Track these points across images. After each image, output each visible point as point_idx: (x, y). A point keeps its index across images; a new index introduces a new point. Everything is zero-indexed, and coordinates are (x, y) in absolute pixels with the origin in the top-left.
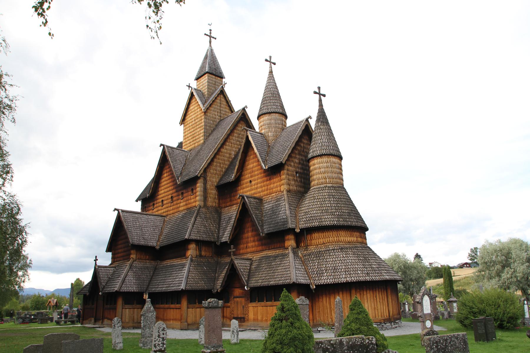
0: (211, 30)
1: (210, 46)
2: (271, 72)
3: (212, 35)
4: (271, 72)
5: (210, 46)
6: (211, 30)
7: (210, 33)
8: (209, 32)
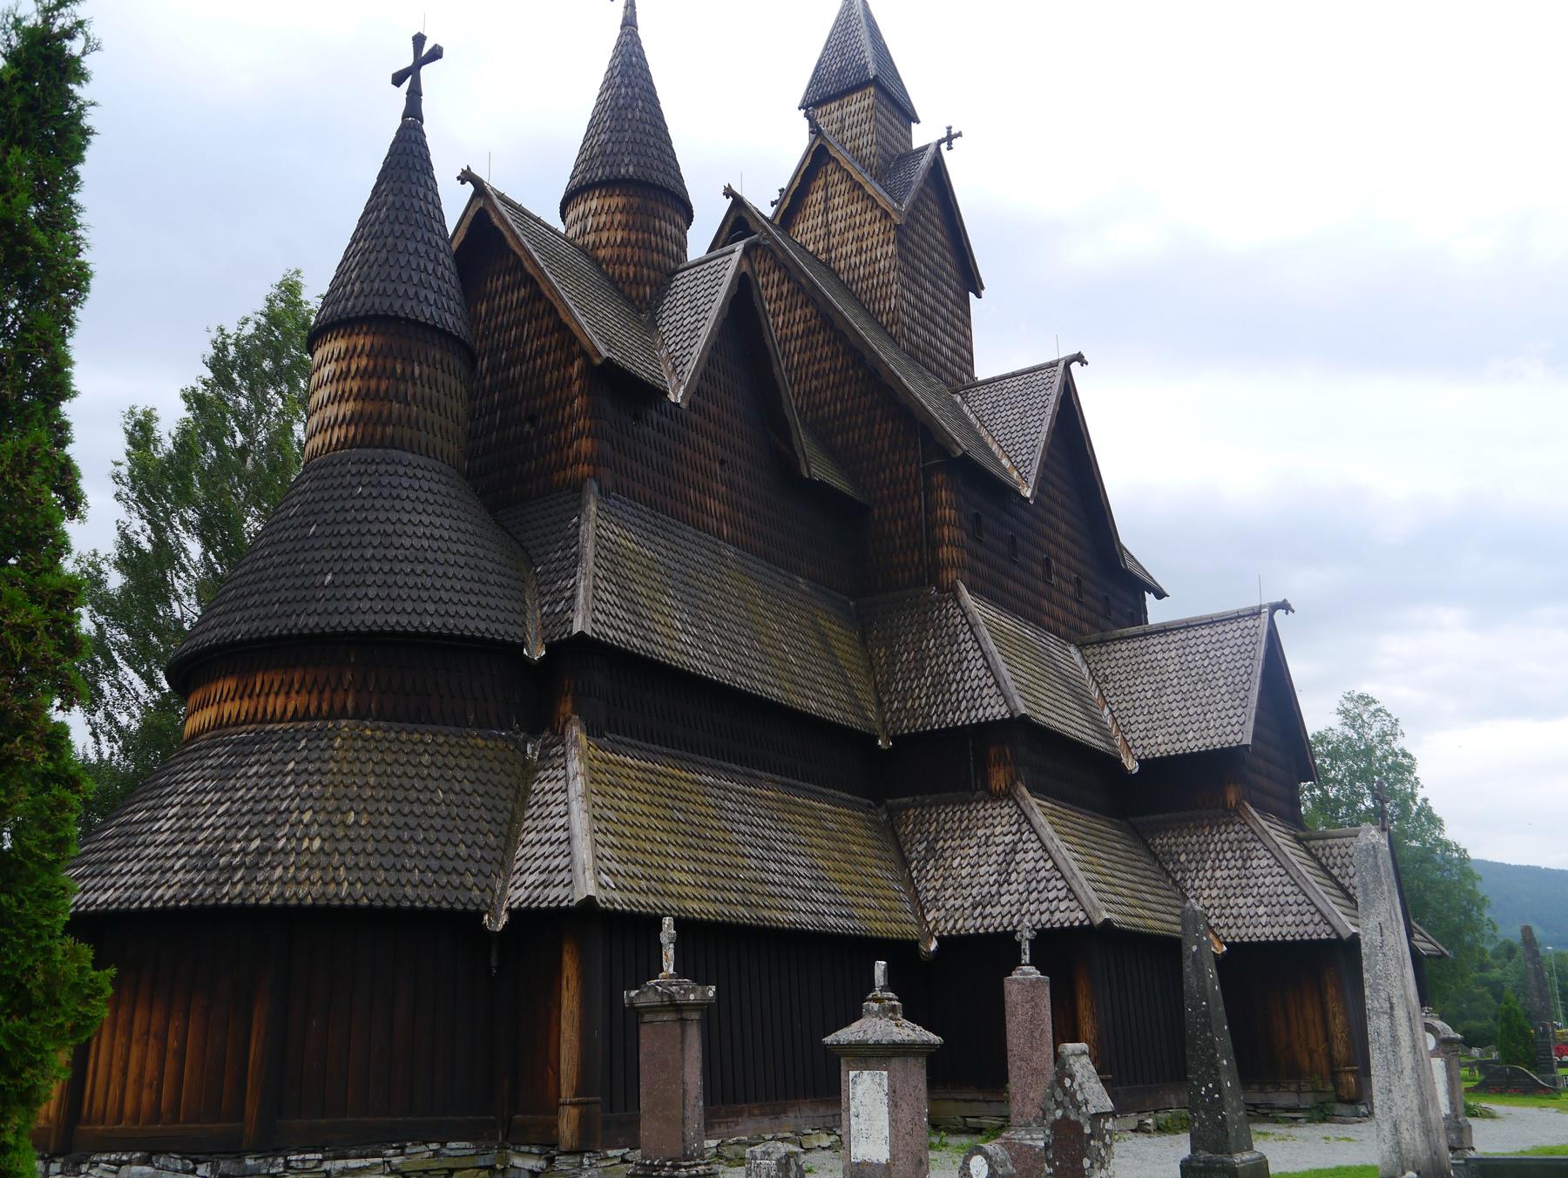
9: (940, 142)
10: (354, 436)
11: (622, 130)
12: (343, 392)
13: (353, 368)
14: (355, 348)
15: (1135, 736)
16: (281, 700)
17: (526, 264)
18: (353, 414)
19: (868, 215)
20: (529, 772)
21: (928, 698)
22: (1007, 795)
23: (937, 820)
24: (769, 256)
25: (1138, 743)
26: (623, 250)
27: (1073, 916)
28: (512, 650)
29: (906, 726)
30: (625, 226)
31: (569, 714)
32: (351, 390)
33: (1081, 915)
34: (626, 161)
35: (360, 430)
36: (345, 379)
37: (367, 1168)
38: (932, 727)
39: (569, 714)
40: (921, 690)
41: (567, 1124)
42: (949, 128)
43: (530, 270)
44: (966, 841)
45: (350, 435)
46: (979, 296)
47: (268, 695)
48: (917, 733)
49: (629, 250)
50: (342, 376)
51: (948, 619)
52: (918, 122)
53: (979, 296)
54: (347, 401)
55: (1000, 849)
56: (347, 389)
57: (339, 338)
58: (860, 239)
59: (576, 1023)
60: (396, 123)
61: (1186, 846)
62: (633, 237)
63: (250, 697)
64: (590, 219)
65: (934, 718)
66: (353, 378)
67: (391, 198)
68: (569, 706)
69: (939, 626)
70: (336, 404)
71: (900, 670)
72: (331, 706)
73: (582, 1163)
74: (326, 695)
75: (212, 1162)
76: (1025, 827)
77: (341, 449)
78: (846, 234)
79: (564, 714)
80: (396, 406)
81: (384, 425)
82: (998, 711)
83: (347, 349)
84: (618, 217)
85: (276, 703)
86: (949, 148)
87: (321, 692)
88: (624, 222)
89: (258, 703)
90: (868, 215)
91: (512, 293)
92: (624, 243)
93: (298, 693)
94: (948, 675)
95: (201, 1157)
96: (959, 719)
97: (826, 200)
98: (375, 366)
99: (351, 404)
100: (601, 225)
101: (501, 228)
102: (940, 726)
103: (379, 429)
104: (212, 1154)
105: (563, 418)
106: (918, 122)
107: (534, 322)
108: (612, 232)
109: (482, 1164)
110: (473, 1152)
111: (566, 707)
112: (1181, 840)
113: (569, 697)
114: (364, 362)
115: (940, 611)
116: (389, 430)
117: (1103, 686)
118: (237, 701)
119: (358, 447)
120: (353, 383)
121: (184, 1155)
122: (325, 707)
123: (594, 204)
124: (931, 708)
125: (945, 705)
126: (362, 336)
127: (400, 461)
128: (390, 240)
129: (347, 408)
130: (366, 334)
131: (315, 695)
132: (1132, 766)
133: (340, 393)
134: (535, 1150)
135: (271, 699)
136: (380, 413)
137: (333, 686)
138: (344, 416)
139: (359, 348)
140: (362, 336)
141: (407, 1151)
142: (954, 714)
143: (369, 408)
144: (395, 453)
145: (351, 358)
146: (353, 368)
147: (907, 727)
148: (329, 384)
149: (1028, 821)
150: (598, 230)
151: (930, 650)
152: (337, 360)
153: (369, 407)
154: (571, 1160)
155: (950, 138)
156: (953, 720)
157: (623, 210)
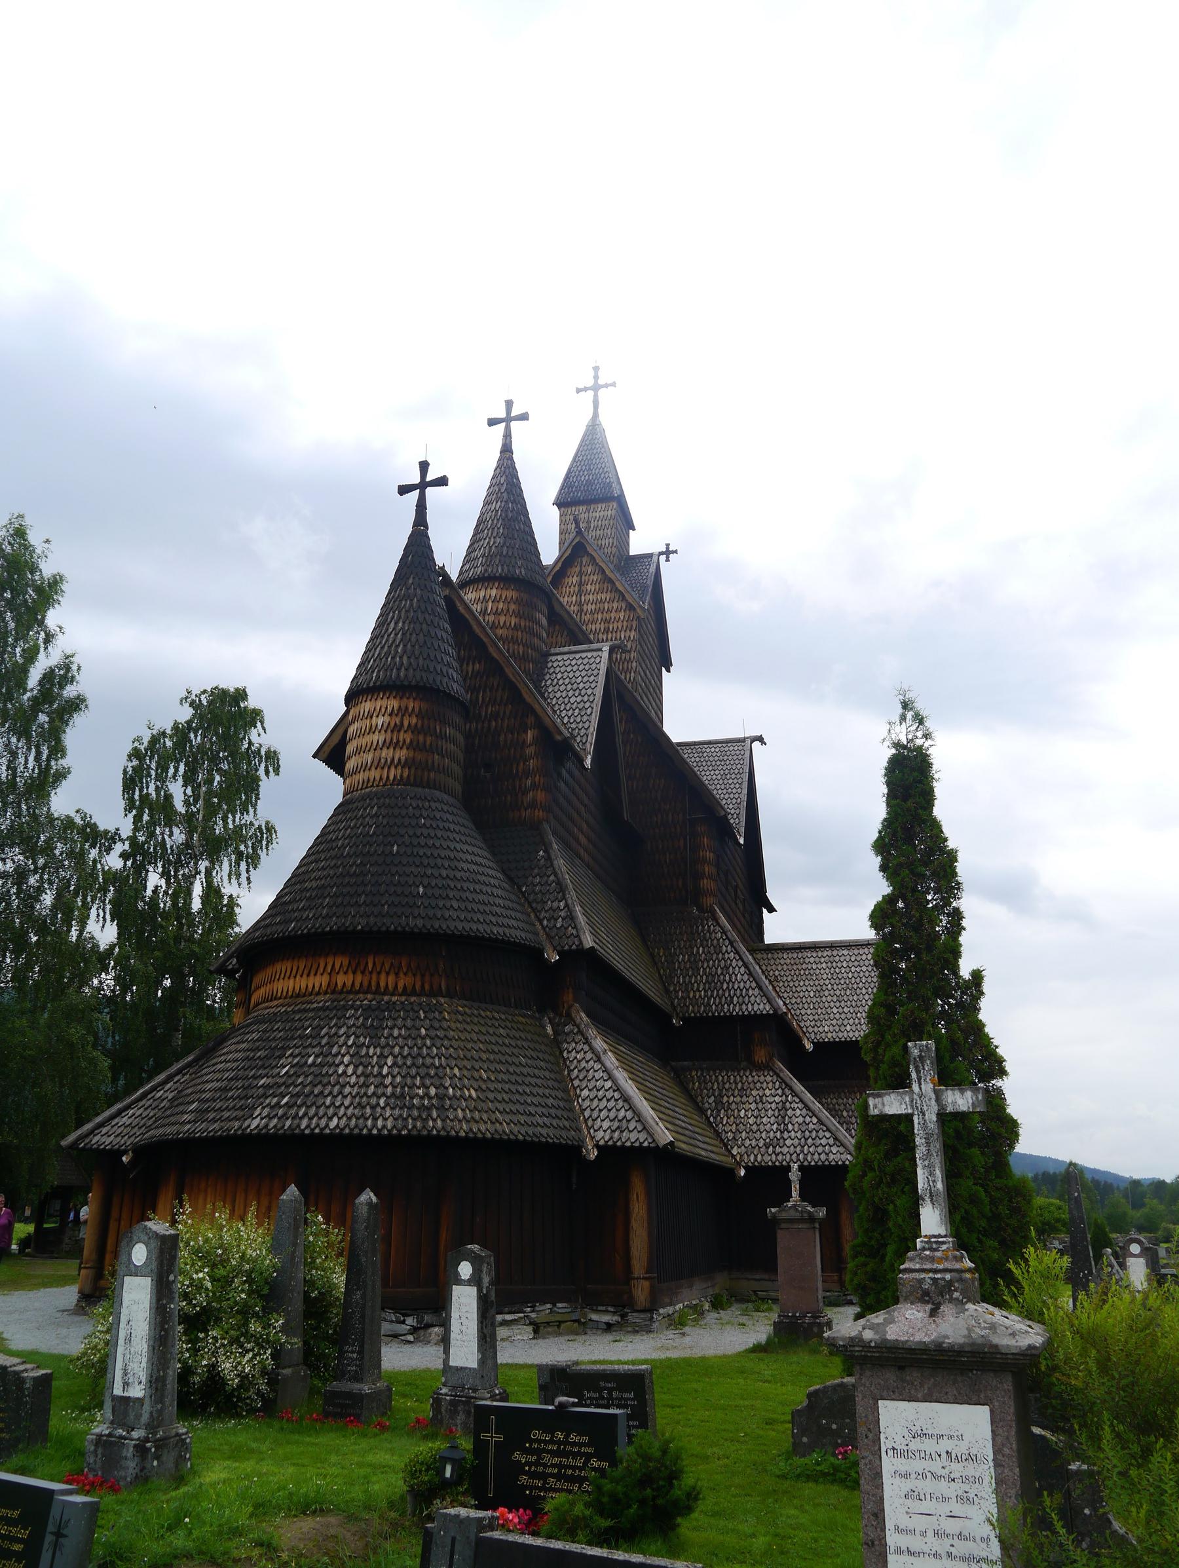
0: (596, 369)
1: (596, 415)
2: (507, 449)
3: (601, 382)
4: (507, 449)
5: (596, 415)
6: (596, 369)
7: (596, 377)
9: (661, 553)
10: (409, 776)
11: (513, 538)
12: (398, 741)
13: (406, 724)
14: (407, 708)
15: (808, 1024)
17: (491, 650)
18: (406, 759)
19: (615, 605)
20: (556, 1044)
21: (706, 991)
22: (767, 1067)
23: (717, 1081)
24: (565, 633)
25: (810, 1030)
26: (515, 632)
27: (844, 1157)
28: (536, 953)
30: (518, 615)
33: (849, 1157)
34: (519, 564)
35: (412, 772)
36: (399, 731)
37: (515, 1320)
38: (713, 1014)
40: (698, 985)
41: (641, 1291)
42: (668, 545)
43: (495, 655)
44: (745, 1099)
46: (668, 671)
47: (379, 973)
48: (702, 1017)
49: (520, 633)
50: (397, 728)
51: (710, 934)
52: (634, 530)
53: (668, 671)
54: (401, 748)
55: (774, 1106)
56: (401, 739)
57: (392, 697)
58: (607, 621)
59: (646, 1224)
61: (845, 1105)
62: (523, 624)
63: (363, 973)
64: (490, 604)
65: (714, 1007)
66: (405, 732)
67: (419, 592)
68: (571, 995)
69: (705, 938)
71: (679, 967)
72: (431, 986)
73: (652, 1318)
74: (427, 978)
75: (418, 1315)
76: (787, 1092)
77: (398, 785)
78: (596, 615)
80: (436, 757)
81: (429, 771)
82: (763, 1007)
84: (512, 606)
86: (667, 560)
87: (423, 976)
88: (517, 611)
90: (615, 605)
91: (468, 664)
92: (517, 628)
93: (405, 974)
94: (719, 976)
96: (734, 1010)
97: (580, 584)
98: (422, 726)
99: (404, 751)
100: (499, 610)
101: (467, 616)
102: (719, 1013)
103: (426, 774)
104: (416, 1310)
105: (517, 771)
106: (634, 530)
107: (488, 693)
109: (574, 1318)
110: (570, 1310)
111: (569, 997)
112: (840, 1101)
113: (571, 990)
114: (414, 721)
115: (703, 927)
116: (432, 775)
117: (775, 984)
118: (351, 976)
119: (411, 785)
121: (396, 1310)
122: (427, 987)
123: (494, 592)
124: (709, 999)
125: (720, 998)
126: (411, 700)
127: (426, 798)
128: (424, 626)
129: (402, 754)
130: (414, 699)
131: (418, 978)
132: (809, 1046)
134: (610, 1309)
135: (383, 976)
136: (427, 761)
137: (405, 970)
138: (400, 759)
139: (410, 709)
140: (411, 700)
141: (537, 1309)
142: (729, 1006)
143: (419, 756)
144: (437, 793)
145: (403, 716)
146: (406, 724)
147: (693, 1011)
148: (383, 732)
149: (791, 1089)
150: (496, 613)
151: (700, 955)
152: (390, 715)
153: (419, 756)
154: (642, 1316)
155: (668, 553)
156: (729, 1010)
157: (518, 601)
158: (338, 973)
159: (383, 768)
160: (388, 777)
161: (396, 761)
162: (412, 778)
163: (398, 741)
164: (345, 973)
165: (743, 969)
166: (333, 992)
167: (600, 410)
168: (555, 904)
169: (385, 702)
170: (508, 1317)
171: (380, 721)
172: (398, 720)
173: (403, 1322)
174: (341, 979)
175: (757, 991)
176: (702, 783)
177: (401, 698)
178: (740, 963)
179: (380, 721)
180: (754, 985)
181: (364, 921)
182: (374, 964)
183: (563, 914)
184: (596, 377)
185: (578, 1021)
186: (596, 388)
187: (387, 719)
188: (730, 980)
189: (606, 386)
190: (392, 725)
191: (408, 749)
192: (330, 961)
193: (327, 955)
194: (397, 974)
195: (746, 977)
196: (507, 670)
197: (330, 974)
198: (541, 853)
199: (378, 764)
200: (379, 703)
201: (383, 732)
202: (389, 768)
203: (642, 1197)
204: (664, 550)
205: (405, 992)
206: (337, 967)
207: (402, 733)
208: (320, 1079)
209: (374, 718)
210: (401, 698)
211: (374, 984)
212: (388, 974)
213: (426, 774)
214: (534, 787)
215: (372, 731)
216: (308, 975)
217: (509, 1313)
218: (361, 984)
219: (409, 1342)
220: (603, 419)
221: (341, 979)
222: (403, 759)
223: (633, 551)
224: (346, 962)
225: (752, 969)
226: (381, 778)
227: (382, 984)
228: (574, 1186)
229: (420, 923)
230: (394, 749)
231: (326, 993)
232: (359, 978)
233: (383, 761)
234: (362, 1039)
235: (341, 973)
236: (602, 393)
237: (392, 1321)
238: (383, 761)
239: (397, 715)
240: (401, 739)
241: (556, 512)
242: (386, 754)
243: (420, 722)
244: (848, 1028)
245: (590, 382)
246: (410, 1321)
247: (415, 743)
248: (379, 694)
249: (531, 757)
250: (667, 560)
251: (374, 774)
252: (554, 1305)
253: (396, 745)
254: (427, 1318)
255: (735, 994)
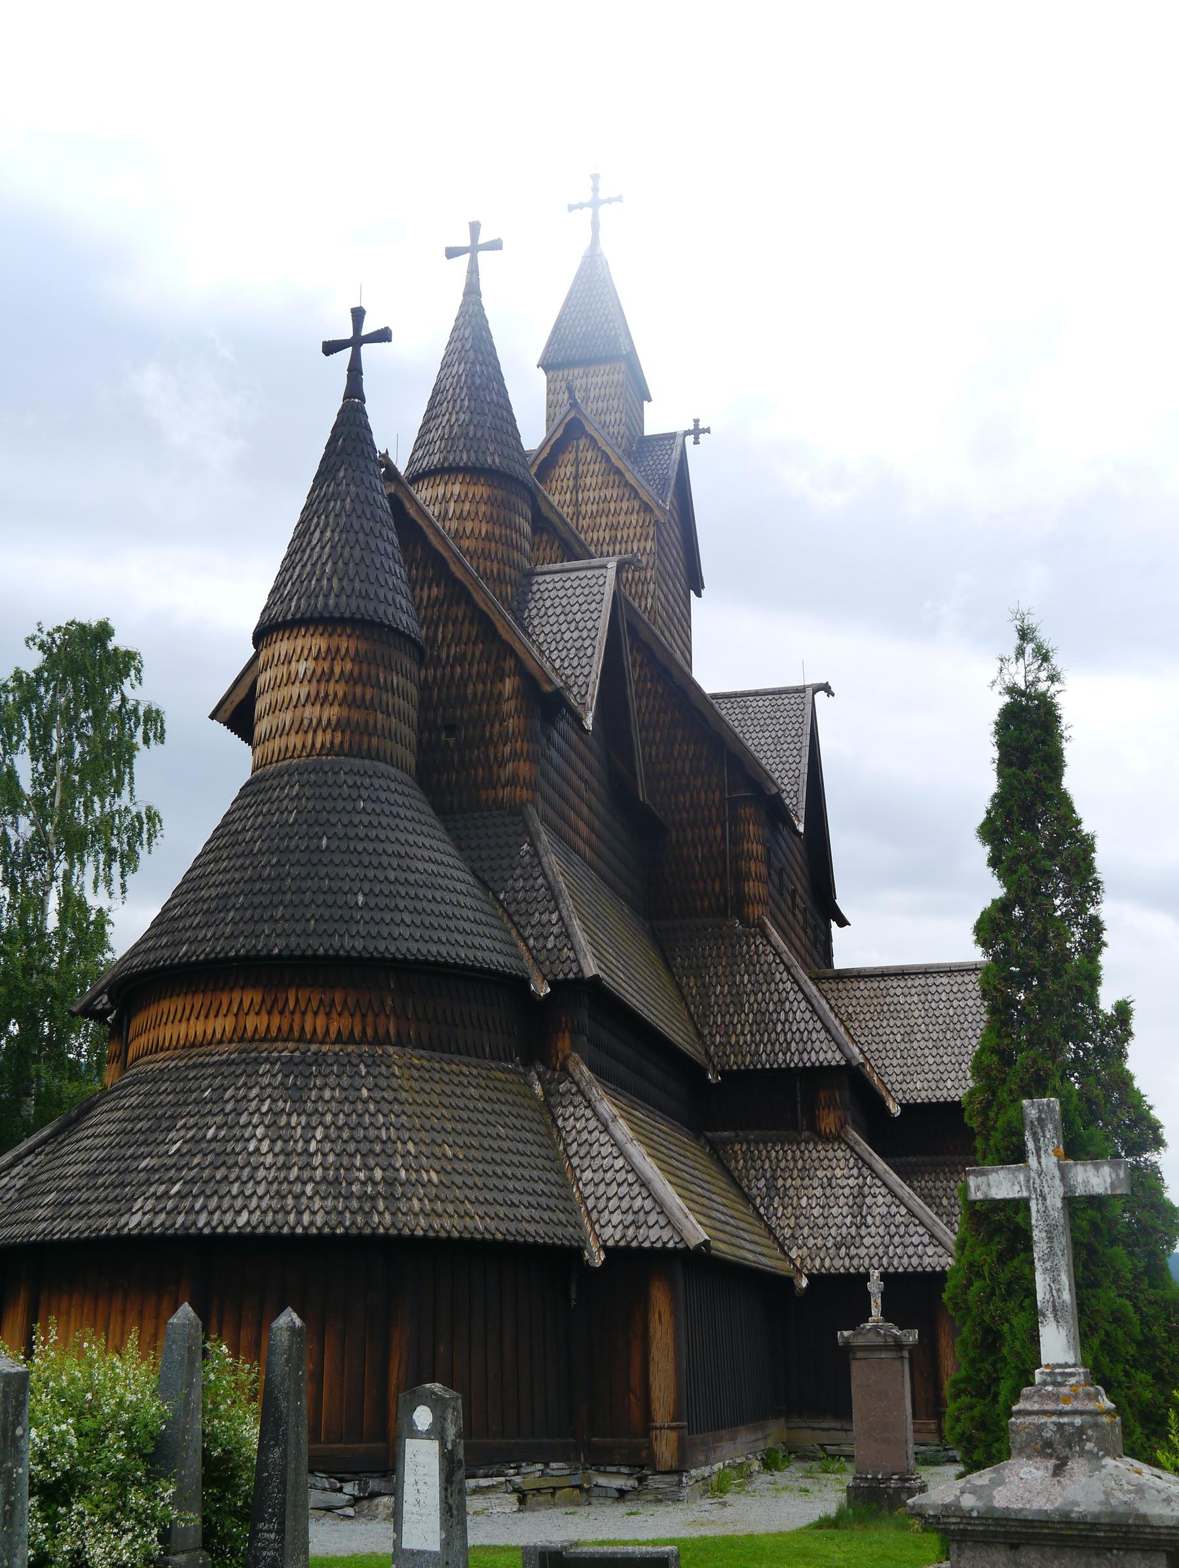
0: (595, 178)
2: (472, 292)
3: (602, 195)
4: (472, 292)
6: (595, 178)
7: (595, 189)
8: (590, 183)
9: (687, 433)
10: (342, 743)
11: (483, 413)
12: (327, 695)
13: (337, 670)
14: (338, 650)
15: (893, 1078)
16: (320, 1022)
17: (454, 568)
18: (339, 720)
19: (625, 505)
20: (548, 1106)
21: (753, 1035)
22: (838, 1138)
23: (768, 1157)
24: (556, 544)
25: (897, 1086)
26: (487, 543)
27: (943, 1261)
29: (733, 1062)
30: (490, 519)
31: (567, 1051)
32: (336, 694)
33: (950, 1260)
34: (491, 449)
35: (347, 738)
36: (328, 681)
37: (493, 1486)
38: (763, 1066)
39: (567, 1051)
40: (743, 1026)
41: (665, 1447)
42: (696, 421)
44: (807, 1182)
45: (337, 741)
46: (699, 595)
47: (304, 1013)
48: (747, 1070)
49: (493, 545)
50: (325, 677)
51: (759, 956)
52: (650, 400)
53: (699, 595)
54: (331, 705)
55: (847, 1191)
56: (331, 692)
57: (317, 634)
58: (614, 527)
59: (671, 1355)
60: (336, 403)
61: (945, 1190)
62: (497, 532)
63: (281, 1013)
64: (452, 504)
65: (764, 1056)
66: (337, 682)
67: (353, 489)
68: (567, 1042)
69: (751, 962)
70: (318, 707)
71: (716, 1003)
73: (681, 1482)
74: (370, 1019)
75: (360, 1481)
76: (866, 1172)
77: (327, 755)
78: (598, 519)
79: (563, 1051)
80: (380, 716)
82: (831, 1056)
83: (329, 649)
84: (483, 508)
85: (316, 1023)
86: (696, 442)
87: (364, 1016)
88: (488, 514)
89: (293, 1020)
90: (625, 505)
91: (422, 589)
92: (489, 537)
93: (340, 1015)
94: (771, 1014)
95: (346, 1476)
96: (792, 1060)
97: (576, 477)
98: (360, 673)
99: (335, 710)
100: (465, 514)
101: (420, 521)
102: (771, 1065)
103: (366, 739)
104: (357, 1473)
106: (650, 400)
107: (451, 627)
108: (477, 522)
109: (574, 1483)
110: (567, 1472)
111: (564, 1043)
112: (938, 1184)
113: (567, 1035)
114: (348, 666)
115: (749, 947)
116: (374, 741)
117: (848, 1024)
118: (265, 1018)
119: (346, 755)
120: (337, 687)
121: (330, 1473)
122: (369, 1032)
123: (457, 489)
124: (757, 1046)
125: (773, 1045)
126: (344, 638)
127: (365, 772)
128: (361, 536)
129: (332, 713)
130: (349, 636)
131: (358, 1018)
132: (895, 1110)
133: (322, 694)
134: (624, 1470)
135: (309, 1017)
136: (367, 722)
137: (339, 1009)
138: (329, 720)
139: (343, 651)
140: (344, 638)
141: (523, 1470)
142: (785, 1054)
143: (356, 715)
144: (381, 766)
145: (333, 659)
146: (337, 670)
147: (735, 1063)
148: (306, 682)
149: (870, 1168)
150: (460, 518)
151: (745, 986)
152: (316, 659)
153: (356, 715)
154: (668, 1479)
155: (697, 432)
156: (785, 1061)
158: (247, 1014)
159: (306, 732)
160: (313, 744)
161: (324, 722)
162: (346, 745)
163: (327, 695)
164: (257, 1014)
165: (803, 1005)
166: (241, 1040)
167: (602, 235)
168: (545, 917)
169: (308, 642)
170: (484, 1482)
171: (302, 665)
172: (326, 666)
173: (340, 1490)
174: (251, 1022)
175: (823, 1035)
176: (746, 750)
177: (330, 635)
178: (800, 996)
179: (302, 665)
180: (819, 1025)
181: (282, 942)
182: (297, 1001)
183: (555, 930)
184: (595, 189)
185: (577, 1077)
186: (595, 204)
187: (311, 664)
188: (787, 1020)
189: (610, 201)
190: (319, 672)
191: (340, 705)
192: (236, 996)
193: (232, 990)
194: (328, 1014)
195: (807, 1015)
196: (475, 595)
197: (236, 1015)
198: (525, 847)
199: (300, 727)
200: (300, 642)
201: (306, 682)
202: (315, 731)
203: (666, 1318)
204: (692, 428)
205: (339, 1039)
206: (246, 1005)
207: (332, 683)
208: (223, 1159)
209: (293, 663)
210: (330, 635)
211: (296, 1028)
212: (316, 1014)
213: (366, 739)
214: (515, 756)
215: (290, 680)
216: (206, 1017)
217: (486, 1476)
218: (279, 1029)
219: (349, 1517)
220: (605, 246)
221: (251, 1022)
222: (334, 719)
223: (650, 429)
224: (258, 999)
225: (816, 1004)
226: (304, 746)
227: (308, 1029)
228: (573, 1303)
229: (359, 944)
230: (322, 705)
231: (231, 1041)
232: (276, 1021)
233: (306, 722)
234: (280, 1104)
235: (252, 1013)
236: (603, 210)
237: (325, 1489)
238: (306, 722)
239: (324, 659)
240: (331, 692)
241: (541, 377)
242: (311, 712)
243: (356, 668)
244: (949, 1084)
245: (587, 197)
246: (350, 1488)
247: (350, 698)
248: (299, 630)
249: (509, 716)
250: (696, 442)
251: (295, 740)
252: (547, 1465)
253: (325, 701)
254: (374, 1484)
255: (793, 1039)
